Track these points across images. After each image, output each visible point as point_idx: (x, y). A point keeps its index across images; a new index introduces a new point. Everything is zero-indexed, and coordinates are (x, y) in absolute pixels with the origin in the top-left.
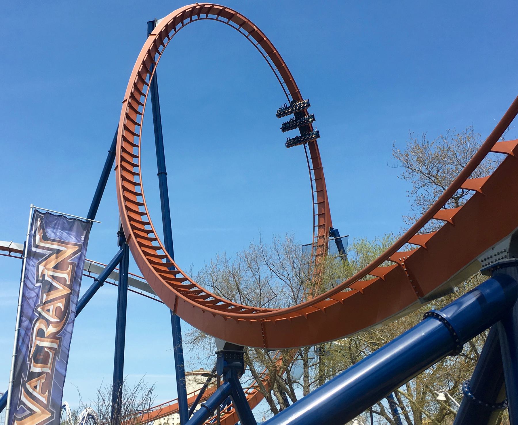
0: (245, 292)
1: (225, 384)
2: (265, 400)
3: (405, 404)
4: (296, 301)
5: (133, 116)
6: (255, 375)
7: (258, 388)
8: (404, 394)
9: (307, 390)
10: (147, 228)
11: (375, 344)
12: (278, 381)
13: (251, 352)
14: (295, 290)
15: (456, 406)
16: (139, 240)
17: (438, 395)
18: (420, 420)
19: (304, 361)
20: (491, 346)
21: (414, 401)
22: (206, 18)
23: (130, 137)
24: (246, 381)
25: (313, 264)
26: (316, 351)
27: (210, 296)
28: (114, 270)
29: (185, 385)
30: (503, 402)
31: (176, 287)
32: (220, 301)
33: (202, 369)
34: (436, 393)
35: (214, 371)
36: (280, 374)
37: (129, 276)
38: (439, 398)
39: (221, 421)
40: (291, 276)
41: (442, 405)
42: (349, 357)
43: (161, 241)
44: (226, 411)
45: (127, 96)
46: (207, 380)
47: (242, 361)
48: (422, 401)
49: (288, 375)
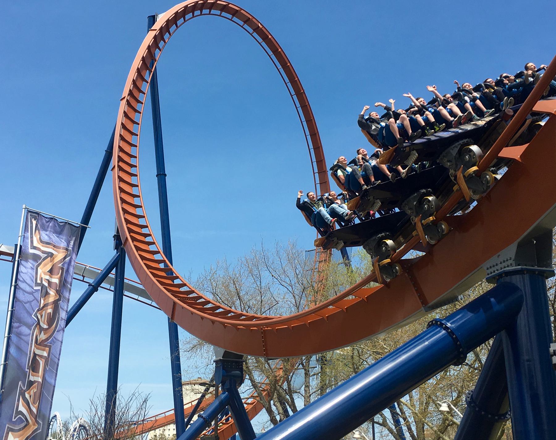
0: (245, 298)
1: (223, 394)
2: (264, 410)
3: (407, 414)
4: (298, 308)
5: (131, 114)
6: (254, 385)
7: (258, 398)
8: (406, 405)
9: (308, 400)
10: (144, 231)
11: (378, 353)
12: (278, 391)
13: (251, 361)
14: (297, 297)
15: (459, 417)
16: (136, 243)
17: (441, 406)
18: (422, 430)
19: (305, 370)
20: (496, 356)
21: (417, 412)
22: (209, 14)
23: (128, 137)
24: (245, 391)
25: (316, 270)
26: (317, 360)
27: (209, 302)
28: (110, 275)
29: (182, 395)
30: (507, 413)
31: (174, 293)
32: (219, 307)
33: (200, 378)
34: (438, 404)
35: (212, 380)
36: (280, 384)
37: (125, 281)
38: (441, 409)
39: (219, 432)
40: (293, 283)
41: (444, 415)
42: (351, 366)
43: (159, 246)
44: (224, 422)
45: (126, 93)
46: (205, 390)
47: (241, 370)
48: (425, 412)
49: (289, 385)
